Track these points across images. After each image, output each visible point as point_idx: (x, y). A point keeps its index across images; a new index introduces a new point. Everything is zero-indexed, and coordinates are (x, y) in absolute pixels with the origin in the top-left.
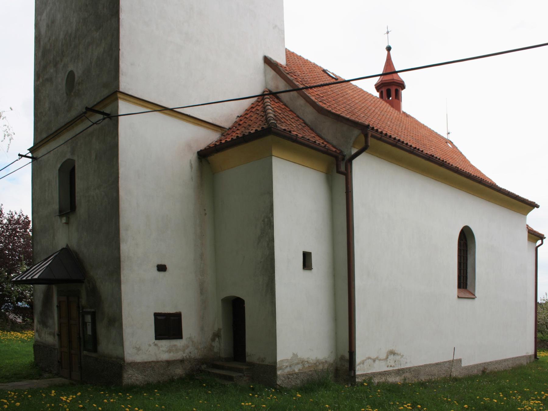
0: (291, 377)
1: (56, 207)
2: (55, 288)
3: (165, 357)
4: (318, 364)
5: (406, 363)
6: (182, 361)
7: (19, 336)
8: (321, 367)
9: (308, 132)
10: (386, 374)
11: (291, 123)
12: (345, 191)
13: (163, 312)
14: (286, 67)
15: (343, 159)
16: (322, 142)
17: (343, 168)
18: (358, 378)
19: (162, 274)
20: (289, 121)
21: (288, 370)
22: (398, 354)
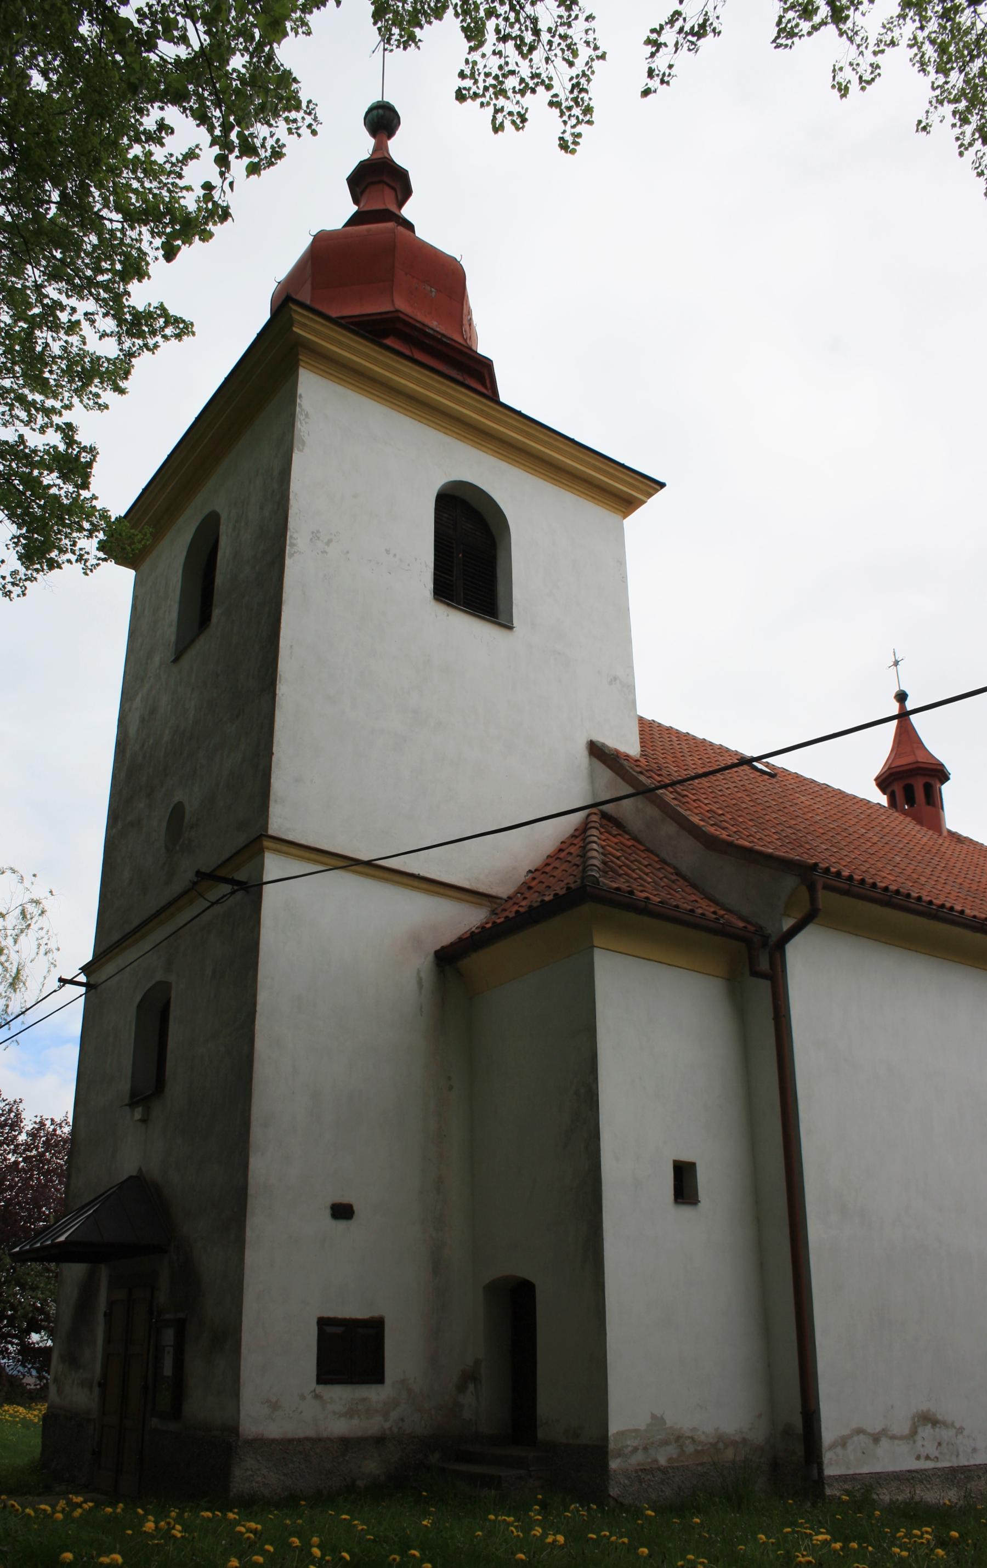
0: (649, 1477)
1: (125, 1086)
2: (104, 1272)
3: (339, 1427)
4: (721, 1445)
5: (974, 1450)
6: (380, 1441)
7: (20, 1414)
8: (729, 1454)
9: (683, 891)
10: (913, 1478)
11: (642, 874)
12: (772, 1015)
13: (340, 1315)
14: (641, 759)
15: (765, 944)
16: (712, 910)
17: (764, 965)
18: (830, 1485)
19: (342, 1225)
20: (637, 871)
21: (638, 1458)
22: (945, 1424)
